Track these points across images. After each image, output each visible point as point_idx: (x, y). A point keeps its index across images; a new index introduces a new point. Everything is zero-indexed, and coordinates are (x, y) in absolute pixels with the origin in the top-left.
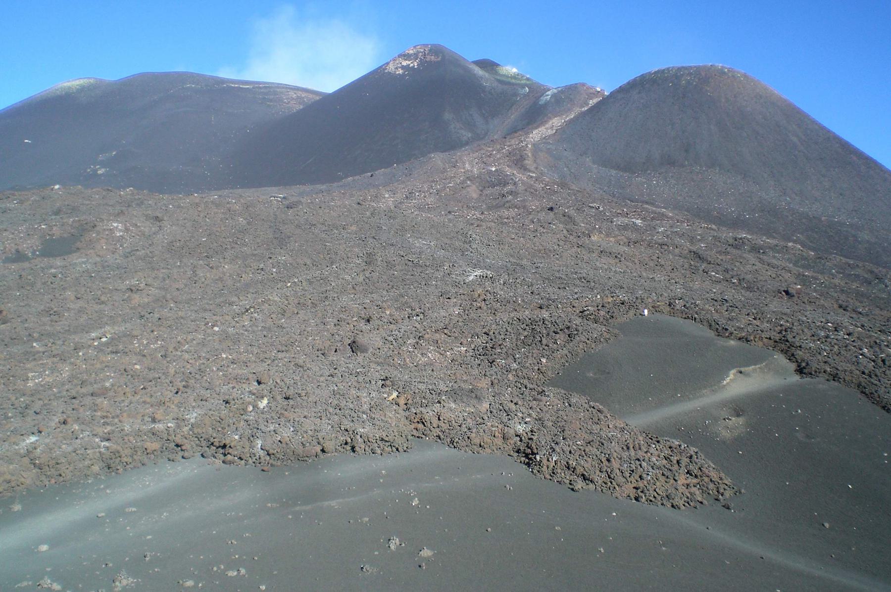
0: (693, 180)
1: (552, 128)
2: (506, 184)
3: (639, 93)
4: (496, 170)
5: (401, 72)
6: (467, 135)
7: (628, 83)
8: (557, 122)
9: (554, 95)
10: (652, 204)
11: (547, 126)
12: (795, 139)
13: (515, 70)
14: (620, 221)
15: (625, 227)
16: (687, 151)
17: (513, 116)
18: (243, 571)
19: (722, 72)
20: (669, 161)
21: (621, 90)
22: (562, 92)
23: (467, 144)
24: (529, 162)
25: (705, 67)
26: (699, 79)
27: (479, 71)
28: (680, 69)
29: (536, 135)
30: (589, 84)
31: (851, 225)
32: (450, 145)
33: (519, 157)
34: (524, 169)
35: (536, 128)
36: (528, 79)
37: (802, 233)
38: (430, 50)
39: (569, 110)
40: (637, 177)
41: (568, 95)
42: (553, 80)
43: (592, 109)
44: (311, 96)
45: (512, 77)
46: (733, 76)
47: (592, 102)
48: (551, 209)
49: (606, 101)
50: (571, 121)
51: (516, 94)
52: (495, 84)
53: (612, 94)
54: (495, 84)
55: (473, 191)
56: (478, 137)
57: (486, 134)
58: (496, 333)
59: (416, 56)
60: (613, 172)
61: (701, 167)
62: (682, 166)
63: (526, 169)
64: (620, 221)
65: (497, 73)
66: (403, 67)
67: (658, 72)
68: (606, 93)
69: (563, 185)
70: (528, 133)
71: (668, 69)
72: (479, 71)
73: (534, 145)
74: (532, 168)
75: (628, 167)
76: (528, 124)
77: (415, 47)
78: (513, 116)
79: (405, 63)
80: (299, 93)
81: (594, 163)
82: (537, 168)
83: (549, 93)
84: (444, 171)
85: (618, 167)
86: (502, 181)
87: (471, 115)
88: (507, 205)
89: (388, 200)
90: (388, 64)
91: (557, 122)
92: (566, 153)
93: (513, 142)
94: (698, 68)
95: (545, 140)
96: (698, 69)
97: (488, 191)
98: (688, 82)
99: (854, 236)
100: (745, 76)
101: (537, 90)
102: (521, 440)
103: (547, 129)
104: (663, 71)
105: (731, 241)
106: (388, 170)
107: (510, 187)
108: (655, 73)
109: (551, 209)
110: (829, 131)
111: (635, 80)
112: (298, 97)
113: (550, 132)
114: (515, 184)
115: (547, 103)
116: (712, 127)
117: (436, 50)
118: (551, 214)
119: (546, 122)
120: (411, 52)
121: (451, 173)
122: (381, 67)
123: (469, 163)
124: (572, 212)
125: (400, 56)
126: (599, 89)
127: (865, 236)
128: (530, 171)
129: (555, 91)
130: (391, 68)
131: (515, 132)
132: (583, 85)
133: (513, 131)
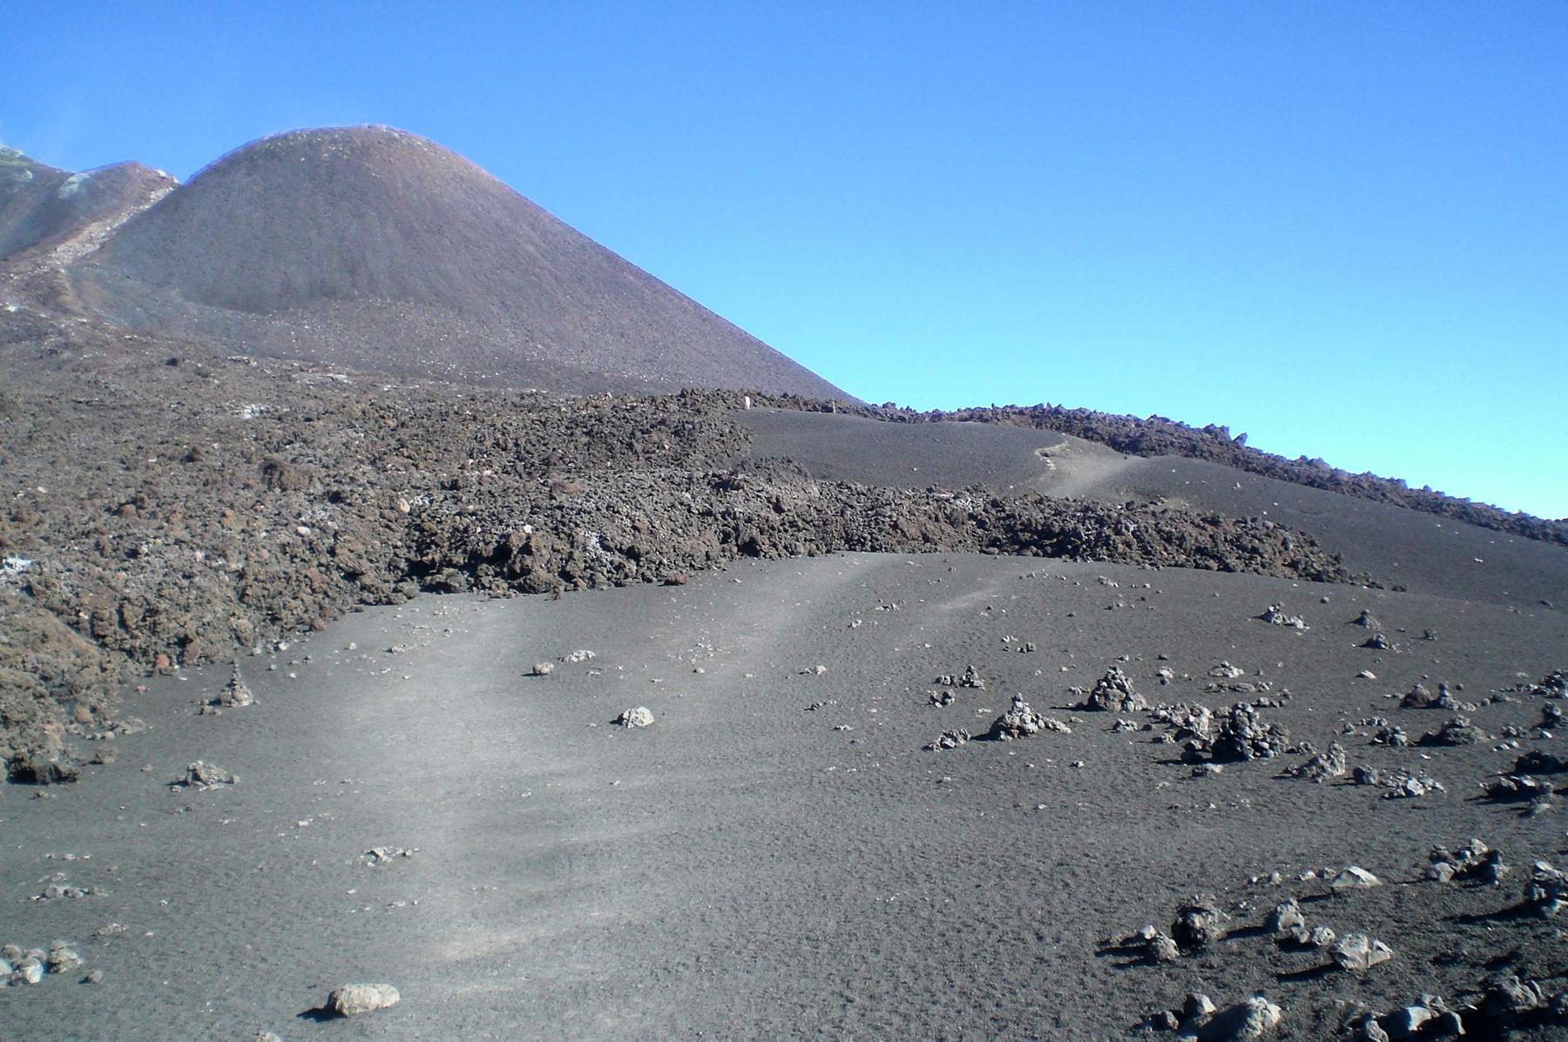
0: (373, 320)
1: (90, 240)
3: (249, 174)
4: (19, 312)
7: (224, 159)
8: (98, 231)
9: (84, 183)
11: (80, 238)
12: (531, 249)
16: (352, 272)
20: (326, 292)
21: (214, 170)
22: (98, 177)
24: (69, 298)
26: (353, 150)
28: (314, 134)
29: (64, 254)
33: (46, 290)
34: (66, 311)
35: (64, 239)
36: (22, 158)
39: (117, 209)
40: (273, 318)
43: (160, 207)
46: (411, 146)
47: (157, 195)
48: (173, 362)
49: (181, 193)
50: (124, 229)
51: (10, 184)
53: (197, 180)
58: (522, 442)
60: (229, 313)
61: (381, 296)
70: (46, 252)
71: (294, 133)
73: (68, 268)
74: (78, 308)
75: (251, 303)
76: (44, 235)
81: (187, 299)
82: (85, 308)
83: (72, 179)
85: (232, 304)
91: (98, 231)
92: (130, 283)
93: (22, 266)
96: (347, 137)
98: (334, 154)
100: (430, 145)
102: (981, 524)
103: (82, 244)
104: (286, 137)
107: (51, 341)
108: (272, 140)
109: (173, 362)
113: (90, 248)
114: (60, 333)
116: (389, 231)
118: (175, 371)
119: (78, 231)
126: (163, 174)
128: (75, 314)
129: (86, 176)
132: (135, 165)
133: (18, 248)
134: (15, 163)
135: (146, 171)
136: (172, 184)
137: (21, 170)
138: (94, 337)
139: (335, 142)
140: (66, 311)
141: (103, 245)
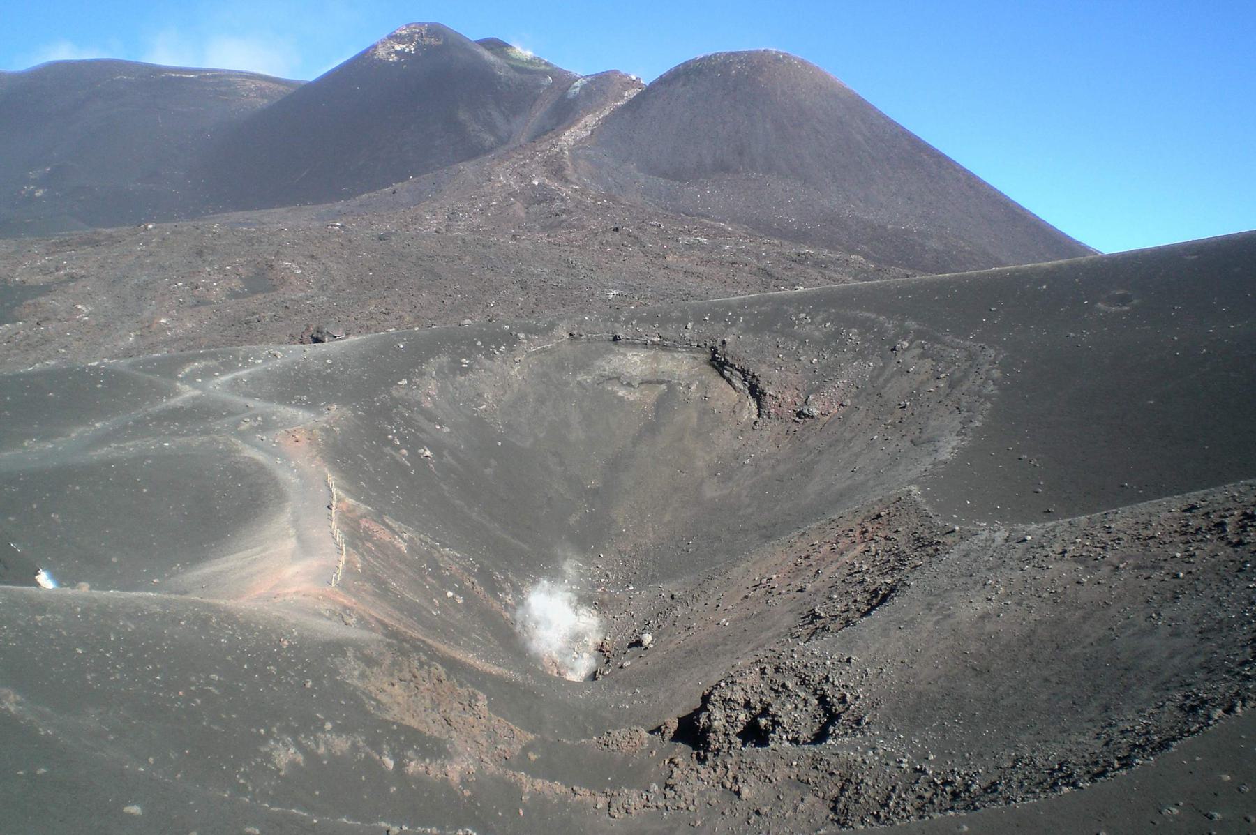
2: (552, 200)
3: (684, 85)
5: (394, 58)
6: (489, 139)
7: (670, 72)
8: (590, 120)
9: (583, 87)
10: (708, 217)
12: (859, 137)
13: (529, 54)
14: (684, 240)
15: (691, 247)
17: (538, 114)
18: (198, 701)
19: (776, 59)
20: (722, 167)
22: (591, 82)
23: (491, 149)
24: (569, 172)
25: (758, 51)
27: (488, 56)
29: (570, 137)
30: (623, 71)
31: (919, 233)
32: (474, 151)
34: (567, 181)
35: (568, 128)
36: (547, 64)
37: (866, 244)
38: (428, 30)
39: (603, 105)
41: (602, 84)
42: (579, 62)
44: (272, 86)
45: (530, 62)
47: (630, 94)
48: (616, 229)
51: (538, 87)
52: (512, 74)
53: (653, 86)
54: (512, 74)
55: (519, 209)
56: (502, 142)
57: (510, 136)
59: (409, 39)
60: (662, 181)
62: (737, 172)
63: (567, 181)
64: (684, 240)
65: (508, 57)
66: (397, 53)
67: (704, 58)
68: (646, 81)
69: (612, 198)
71: (715, 55)
72: (488, 56)
74: (574, 179)
75: (677, 174)
76: (558, 124)
77: (408, 26)
78: (538, 114)
79: (398, 48)
80: (258, 83)
84: (479, 186)
85: (665, 175)
86: (546, 196)
87: (489, 114)
88: (563, 225)
89: (432, 223)
90: (375, 47)
91: (590, 120)
94: (749, 53)
95: (580, 143)
97: (535, 209)
99: (920, 245)
100: (803, 62)
101: (563, 80)
105: (795, 257)
106: (406, 184)
109: (616, 229)
110: (897, 125)
111: (677, 69)
112: (258, 89)
113: (585, 134)
114: (562, 199)
115: (577, 97)
117: (435, 30)
120: (404, 32)
121: (487, 188)
122: (365, 52)
123: (504, 178)
124: (636, 233)
125: (391, 37)
127: (933, 244)
130: (381, 53)
131: (545, 133)
132: (616, 72)
133: (540, 134)
134: (543, 68)
135: (622, 76)
136: (640, 86)
137: (545, 74)
138: (581, 202)
139: (741, 62)
140: (567, 181)
141: (592, 131)
